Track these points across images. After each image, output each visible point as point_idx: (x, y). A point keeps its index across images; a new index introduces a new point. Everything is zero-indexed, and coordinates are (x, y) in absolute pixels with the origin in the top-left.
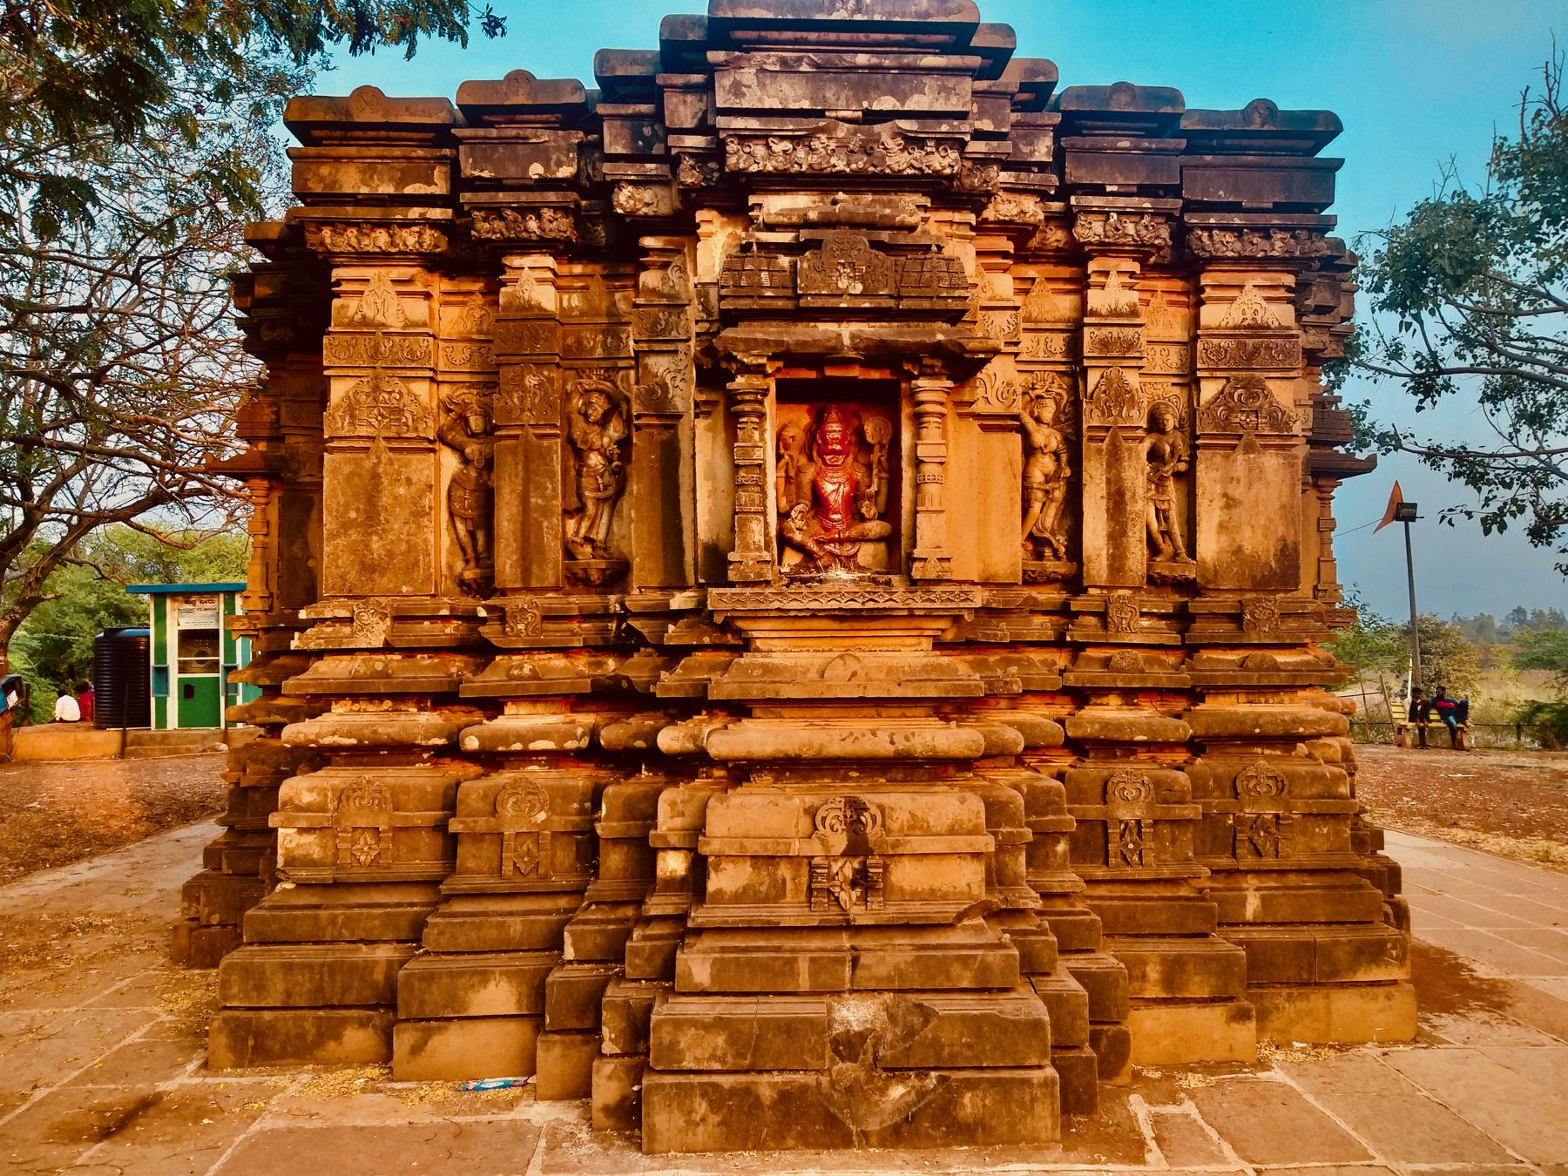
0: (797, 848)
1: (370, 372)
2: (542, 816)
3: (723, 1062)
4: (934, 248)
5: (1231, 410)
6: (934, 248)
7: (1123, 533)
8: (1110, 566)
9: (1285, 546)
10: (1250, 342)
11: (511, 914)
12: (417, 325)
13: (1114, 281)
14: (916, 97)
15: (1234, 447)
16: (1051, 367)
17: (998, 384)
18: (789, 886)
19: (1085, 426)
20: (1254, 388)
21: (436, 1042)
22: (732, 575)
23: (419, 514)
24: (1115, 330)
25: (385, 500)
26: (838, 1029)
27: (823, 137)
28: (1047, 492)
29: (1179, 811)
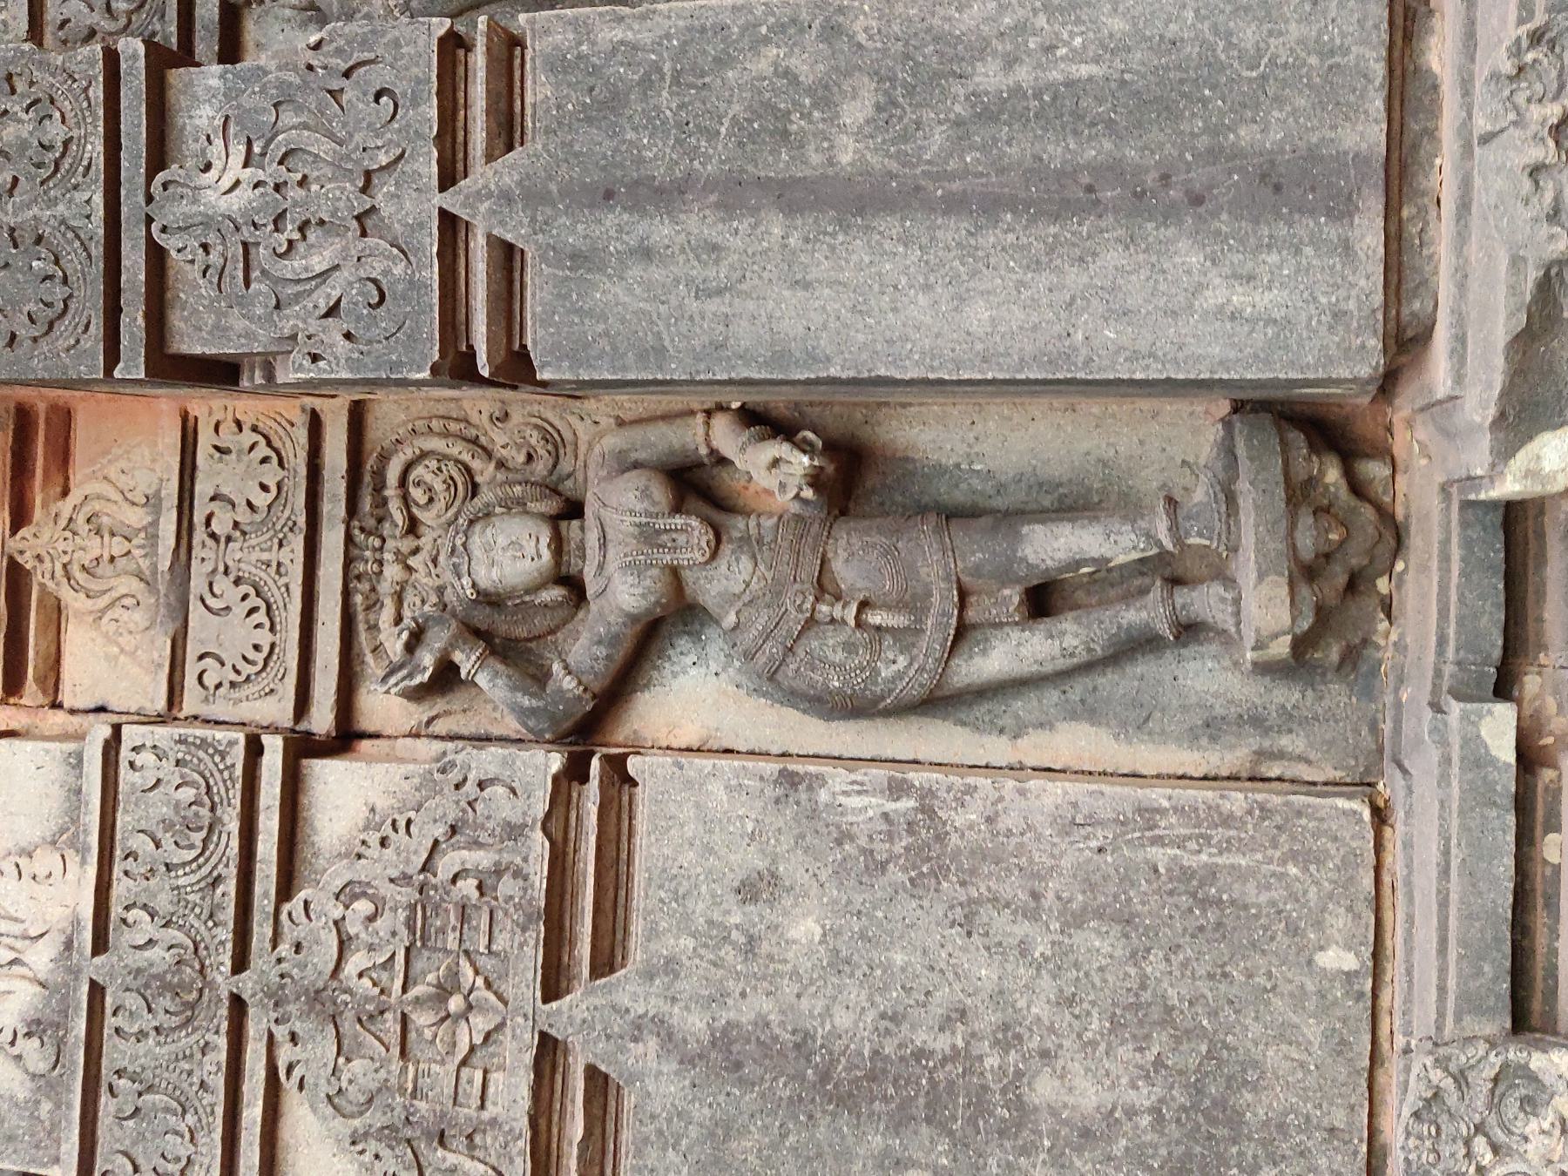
1: (255, 1028)
23: (925, 849)
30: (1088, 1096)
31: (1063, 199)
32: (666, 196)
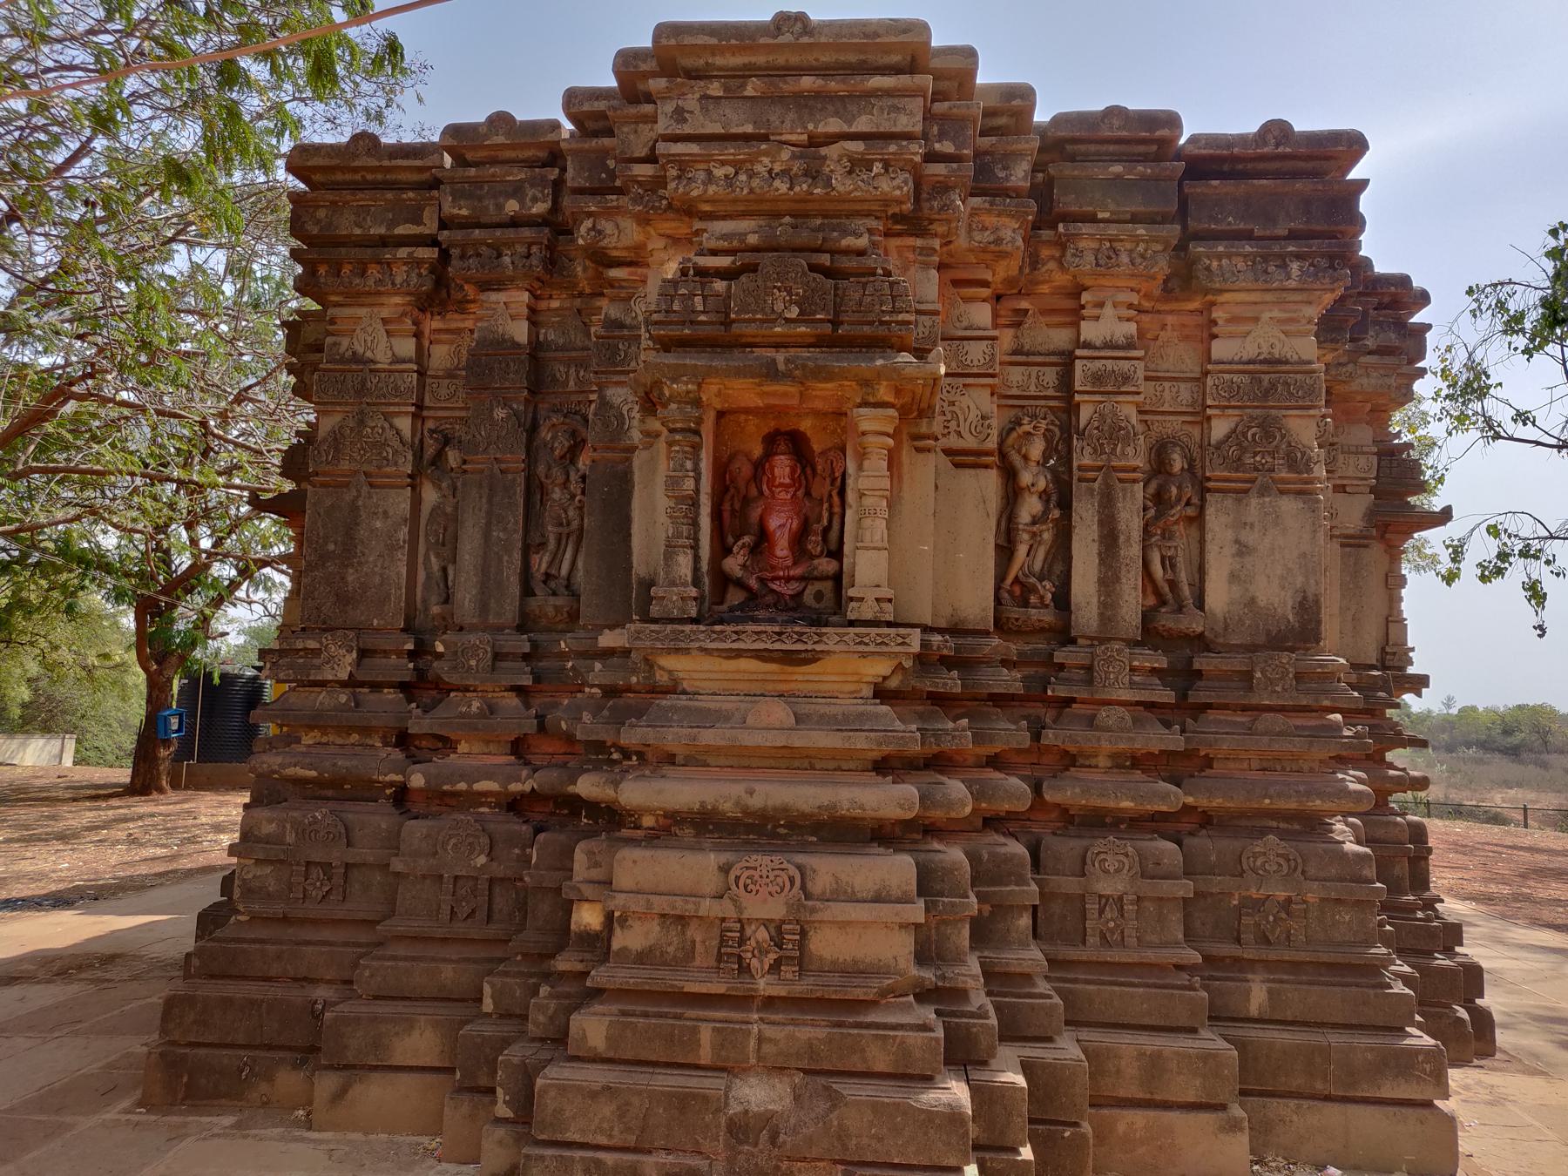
0: (708, 907)
2: (482, 860)
3: (610, 1136)
4: (880, 271)
5: (1243, 450)
6: (880, 271)
7: (1118, 579)
8: (1101, 615)
9: (1305, 598)
10: (1266, 378)
11: (444, 960)
12: (404, 361)
13: (1108, 311)
14: (864, 118)
15: (1246, 491)
16: (1043, 402)
17: (972, 417)
18: (699, 948)
19: (1075, 464)
20: (1269, 429)
21: (357, 1090)
22: (655, 610)
23: (393, 548)
24: (1109, 363)
25: (362, 533)
26: (734, 1109)
27: (766, 160)
28: (1034, 535)
29: (1168, 888)
30: (350, 579)
31: (484, 570)
32: (490, 501)
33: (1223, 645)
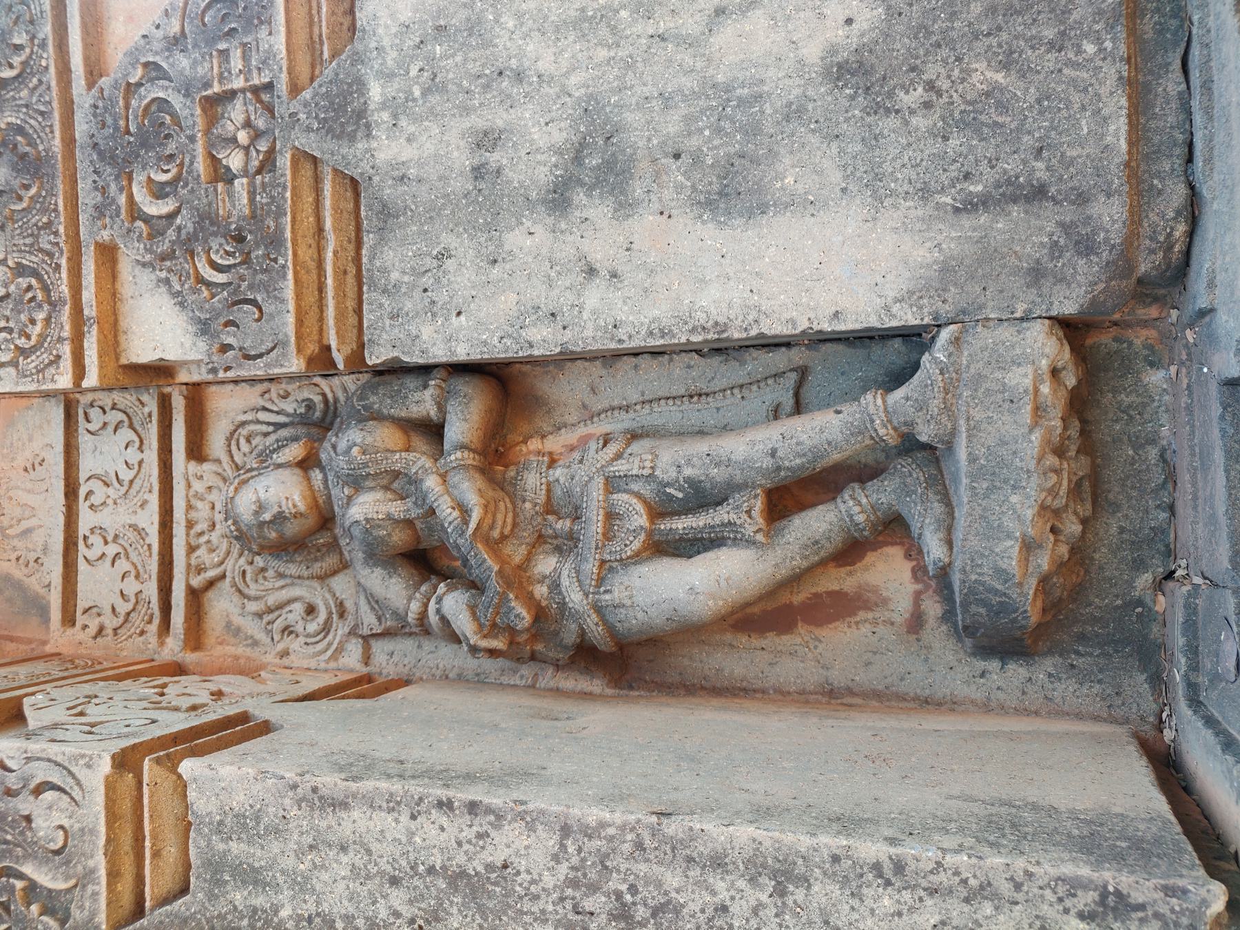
5: (208, 221)
33: (1140, 191)
